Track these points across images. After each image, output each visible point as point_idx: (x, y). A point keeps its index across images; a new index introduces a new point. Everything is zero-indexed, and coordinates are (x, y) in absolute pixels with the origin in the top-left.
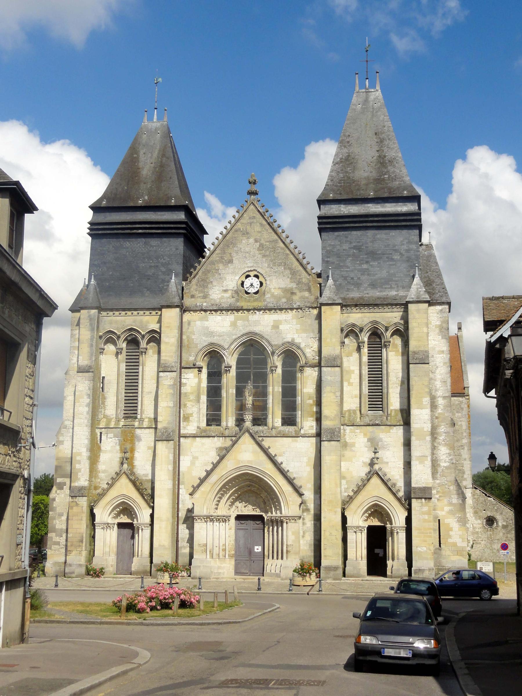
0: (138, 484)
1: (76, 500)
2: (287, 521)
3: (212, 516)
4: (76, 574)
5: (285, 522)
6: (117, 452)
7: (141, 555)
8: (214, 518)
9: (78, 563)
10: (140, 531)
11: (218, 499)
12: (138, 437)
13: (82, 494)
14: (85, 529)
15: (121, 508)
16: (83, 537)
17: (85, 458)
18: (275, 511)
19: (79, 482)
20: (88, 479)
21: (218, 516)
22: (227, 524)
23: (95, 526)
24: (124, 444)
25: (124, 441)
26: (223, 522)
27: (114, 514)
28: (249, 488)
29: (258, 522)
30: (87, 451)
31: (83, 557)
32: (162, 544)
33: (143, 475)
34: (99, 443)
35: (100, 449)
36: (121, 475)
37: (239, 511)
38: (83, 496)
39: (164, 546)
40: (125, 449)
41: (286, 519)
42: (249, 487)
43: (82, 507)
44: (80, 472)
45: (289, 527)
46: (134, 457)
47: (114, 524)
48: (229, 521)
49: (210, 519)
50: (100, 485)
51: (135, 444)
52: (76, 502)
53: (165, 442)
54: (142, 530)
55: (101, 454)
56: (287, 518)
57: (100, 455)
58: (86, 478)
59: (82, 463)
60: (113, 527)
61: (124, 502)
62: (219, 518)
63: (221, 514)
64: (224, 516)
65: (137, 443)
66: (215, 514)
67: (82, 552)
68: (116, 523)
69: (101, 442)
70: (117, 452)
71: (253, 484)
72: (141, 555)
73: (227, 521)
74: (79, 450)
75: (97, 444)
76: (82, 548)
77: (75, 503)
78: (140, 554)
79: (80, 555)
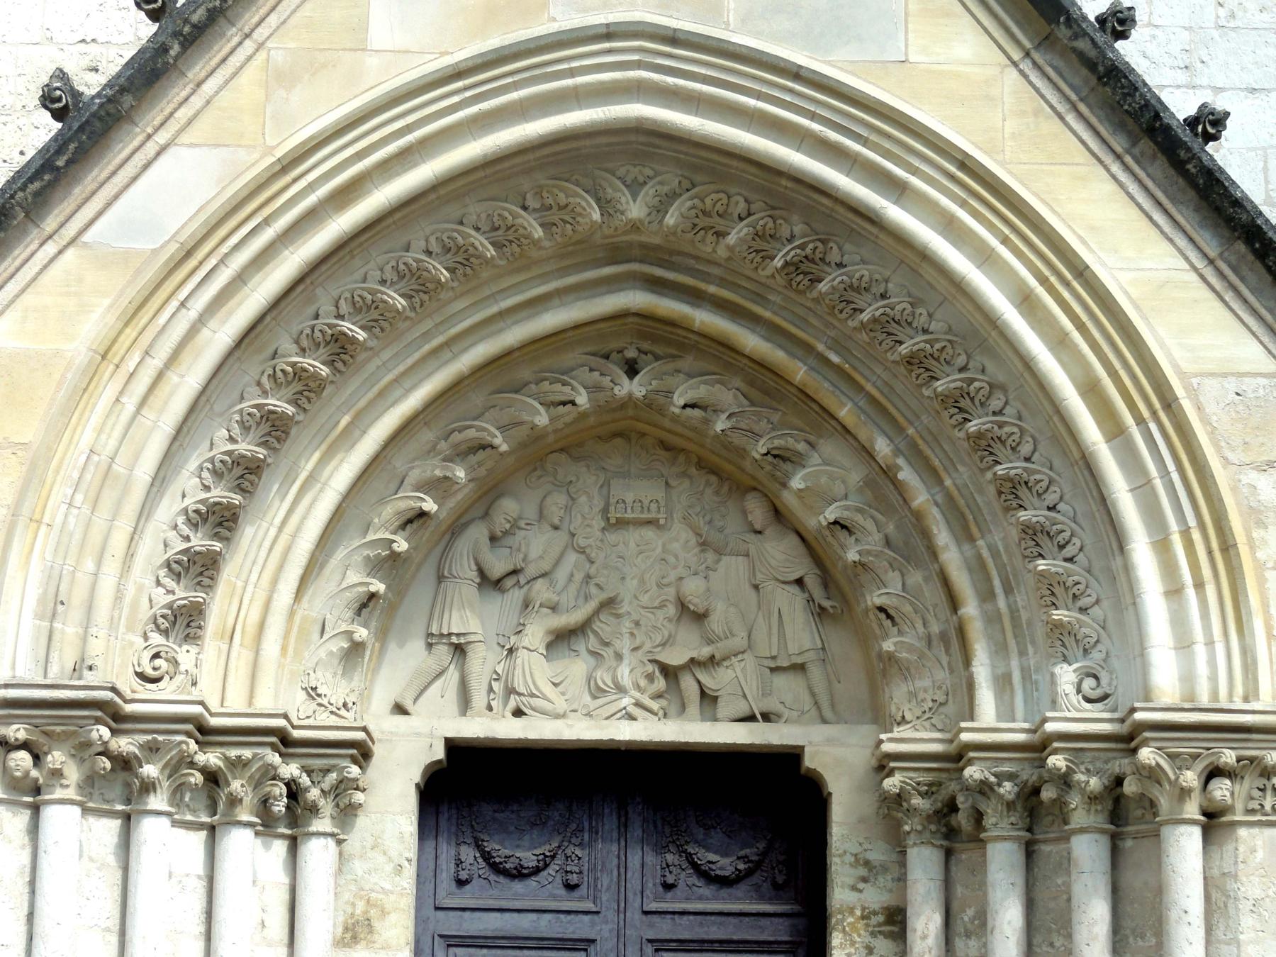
2: (1222, 789)
3: (118, 719)
5: (1192, 809)
8: (152, 749)
11: (219, 493)
18: (1003, 683)
21: (205, 733)
22: (317, 853)
26: (266, 824)
28: (635, 388)
29: (725, 865)
37: (479, 699)
41: (1214, 773)
42: (632, 370)
45: (1250, 887)
48: (347, 813)
49: (82, 749)
56: (1228, 757)
62: (212, 758)
63: (236, 702)
64: (285, 742)
66: (166, 689)
71: (704, 318)
73: (322, 824)
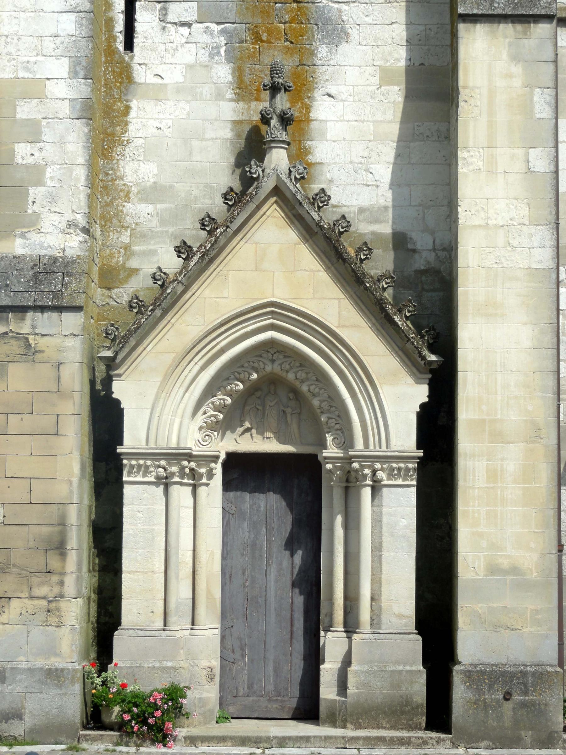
0: (351, 252)
1: (25, 328)
4: (29, 721)
6: (219, 96)
7: (375, 621)
9: (39, 663)
10: (367, 493)
12: (327, 21)
13: (56, 294)
14: (75, 481)
15: (255, 376)
16: (62, 523)
17: (65, 109)
19: (34, 237)
20: (81, 220)
23: (119, 469)
24: (255, 57)
25: (257, 38)
27: (217, 409)
30: (74, 74)
31: (65, 632)
32: (505, 563)
33: (361, 210)
34: (121, 47)
35: (130, 79)
36: (258, 208)
38: (60, 309)
39: (514, 570)
40: (274, 70)
43: (60, 364)
44: (40, 183)
46: (308, 120)
47: (215, 458)
50: (133, 263)
51: (312, 54)
52: (18, 336)
53: (507, 29)
54: (376, 488)
55: (134, 104)
57: (128, 109)
58: (69, 216)
59: (48, 135)
60: (210, 475)
61: (272, 343)
65: (323, 51)
67: (63, 604)
68: (223, 456)
69: (129, 45)
70: (219, 96)
72: (375, 621)
74: (27, 69)
75: (111, 51)
76: (62, 583)
77: (15, 347)
78: (365, 614)
79: (53, 620)
